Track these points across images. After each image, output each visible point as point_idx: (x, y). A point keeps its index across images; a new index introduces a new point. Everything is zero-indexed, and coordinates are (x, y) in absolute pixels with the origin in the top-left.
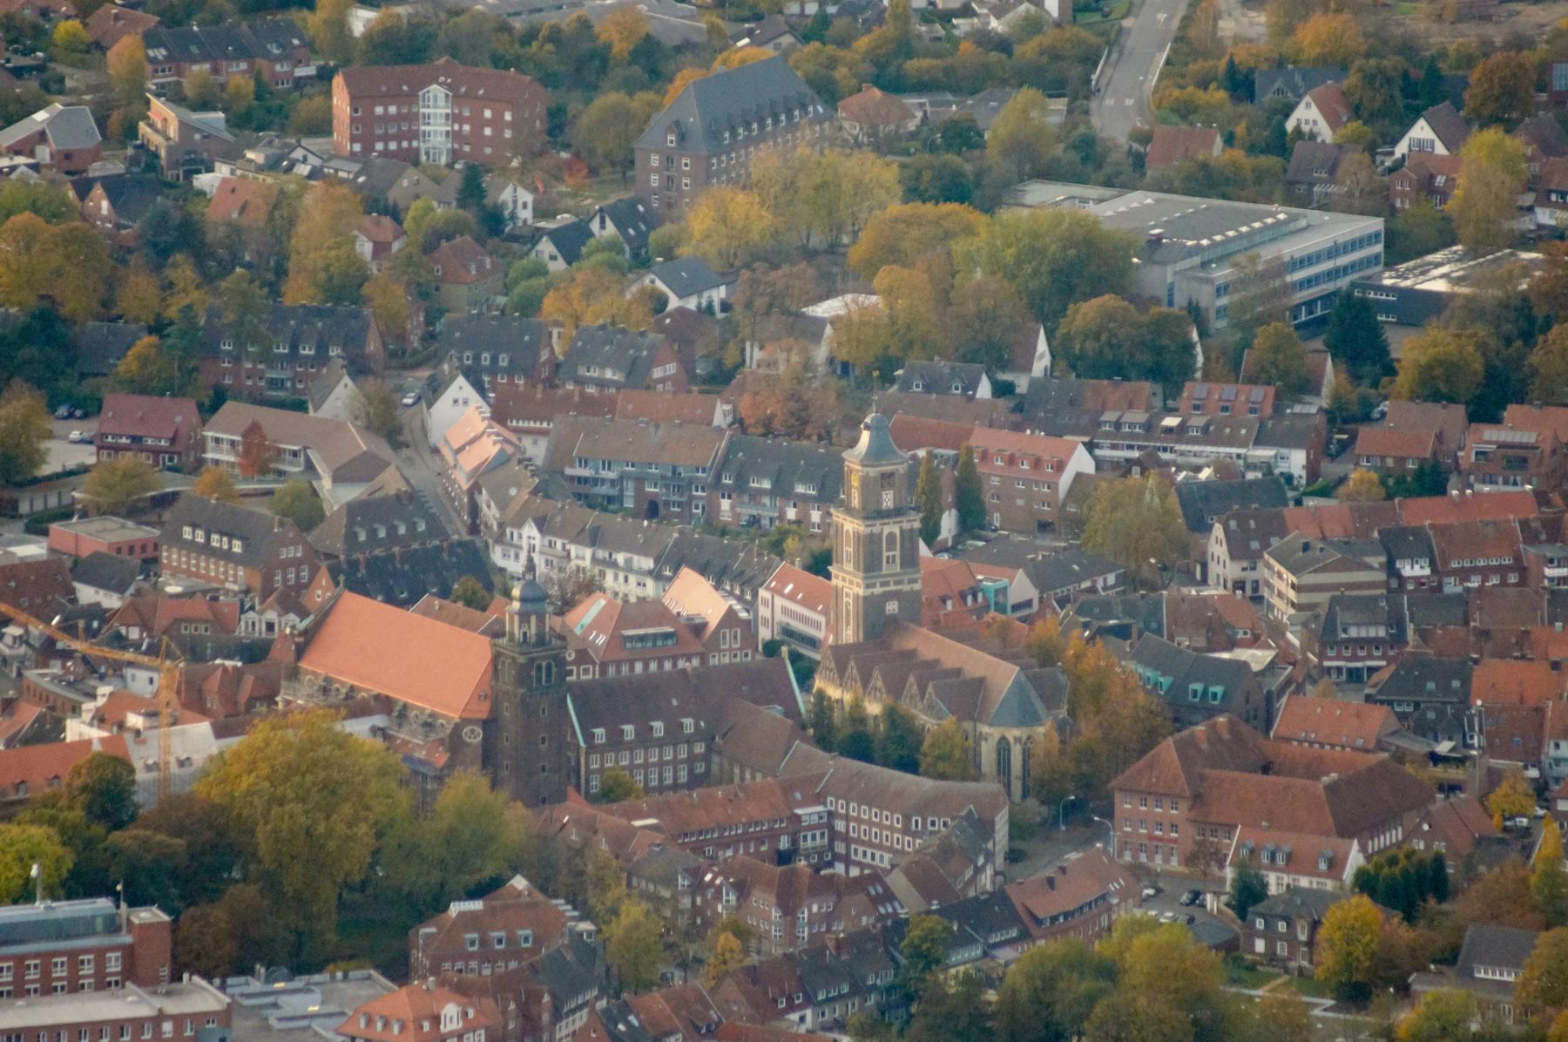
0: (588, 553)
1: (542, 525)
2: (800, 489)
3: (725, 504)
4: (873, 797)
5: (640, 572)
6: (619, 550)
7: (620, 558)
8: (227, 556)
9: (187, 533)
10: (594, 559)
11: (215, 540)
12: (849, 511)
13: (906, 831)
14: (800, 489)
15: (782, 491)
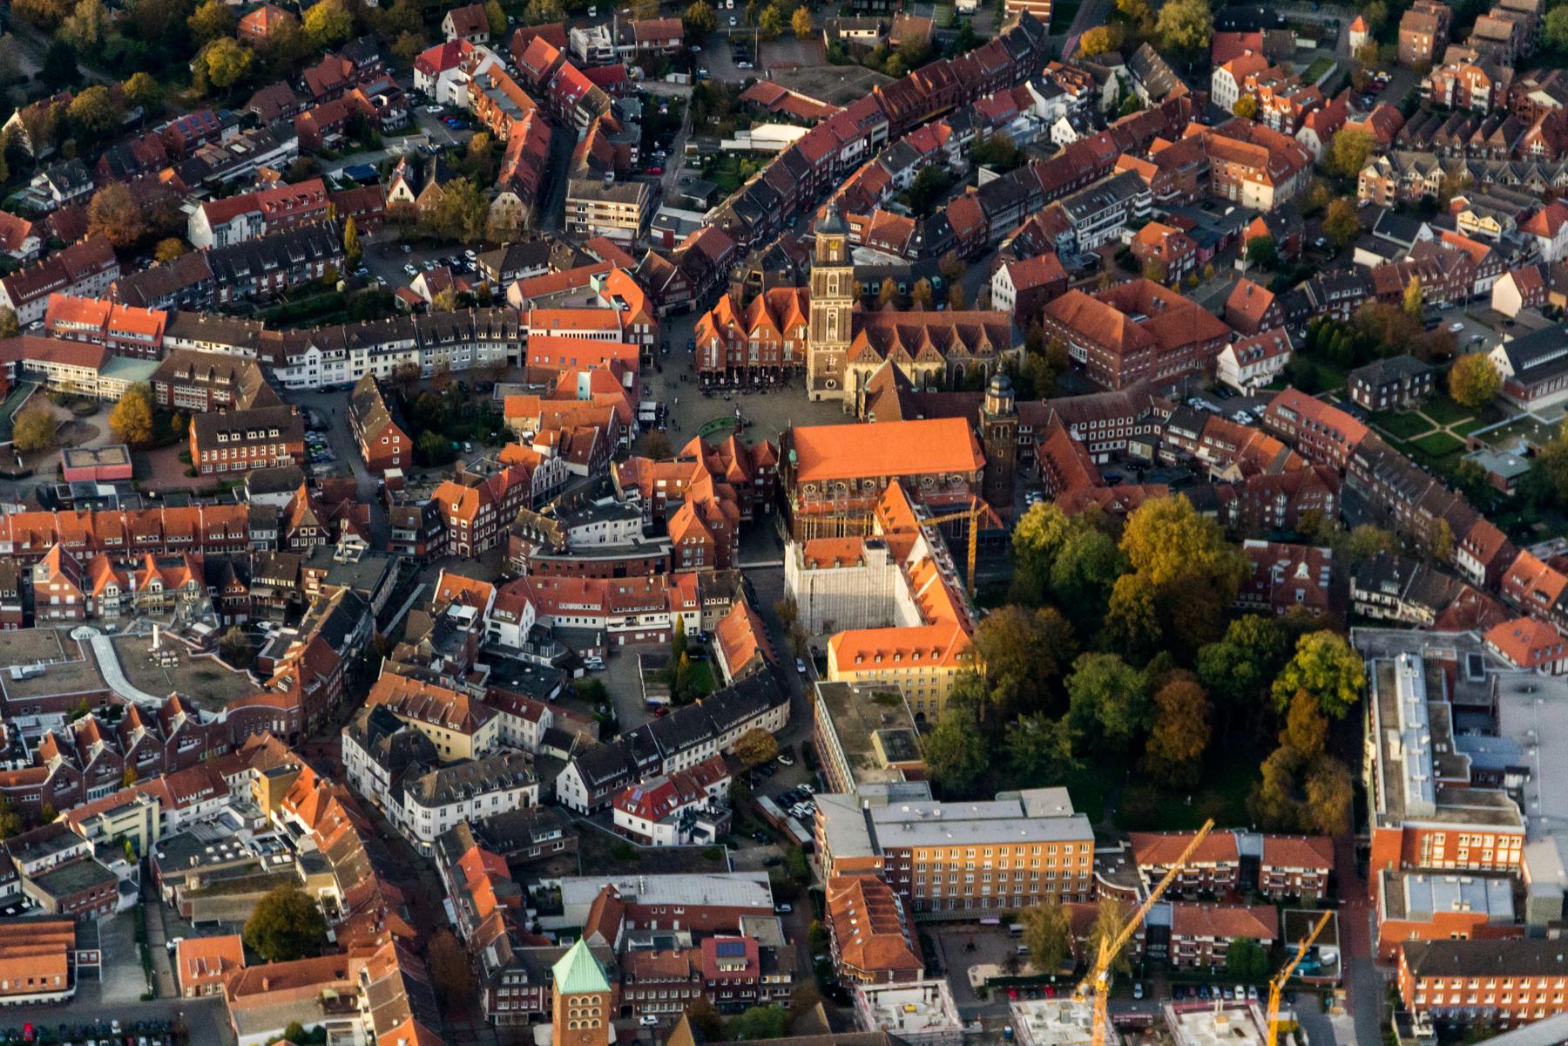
0: (366, 351)
1: (321, 347)
2: (268, 267)
3: (224, 292)
4: (1101, 413)
5: (401, 350)
6: (383, 342)
7: (385, 347)
8: (268, 441)
9: (222, 439)
10: (370, 354)
11: (252, 436)
12: (828, 264)
13: (1136, 424)
14: (268, 267)
15: (258, 272)
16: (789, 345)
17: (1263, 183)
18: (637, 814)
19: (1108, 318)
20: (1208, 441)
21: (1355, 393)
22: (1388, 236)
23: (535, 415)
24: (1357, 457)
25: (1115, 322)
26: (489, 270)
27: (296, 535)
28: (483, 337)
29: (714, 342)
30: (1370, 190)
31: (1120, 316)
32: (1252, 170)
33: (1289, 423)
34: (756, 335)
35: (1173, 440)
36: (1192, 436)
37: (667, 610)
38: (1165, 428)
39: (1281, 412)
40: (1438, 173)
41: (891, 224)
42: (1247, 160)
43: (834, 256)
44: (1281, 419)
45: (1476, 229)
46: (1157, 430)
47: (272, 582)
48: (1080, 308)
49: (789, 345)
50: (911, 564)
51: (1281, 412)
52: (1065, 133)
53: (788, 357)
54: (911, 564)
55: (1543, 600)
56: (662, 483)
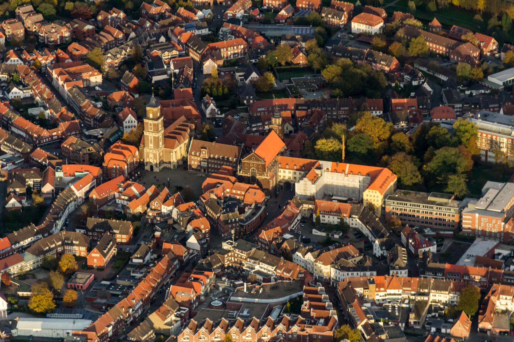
16: (135, 159)
17: (98, 75)
18: (427, 246)
19: (186, 110)
20: (267, 123)
21: (245, 102)
22: (155, 70)
23: (138, 206)
24: (300, 108)
25: (190, 110)
26: (17, 190)
27: (185, 257)
28: (69, 201)
29: (126, 167)
30: (110, 67)
31: (189, 107)
32: (91, 73)
33: (264, 111)
34: (129, 160)
35: (254, 129)
36: (261, 124)
37: (297, 217)
38: (251, 127)
39: (259, 110)
40: (124, 52)
41: (69, 126)
42: (87, 71)
43: (159, 115)
44: (260, 112)
45: (169, 57)
46: (248, 128)
47: (215, 267)
48: (173, 113)
49: (135, 159)
50: (328, 169)
51: (259, 110)
52: (16, 93)
53: (135, 164)
54: (328, 169)
55: (414, 108)
56: (222, 194)
